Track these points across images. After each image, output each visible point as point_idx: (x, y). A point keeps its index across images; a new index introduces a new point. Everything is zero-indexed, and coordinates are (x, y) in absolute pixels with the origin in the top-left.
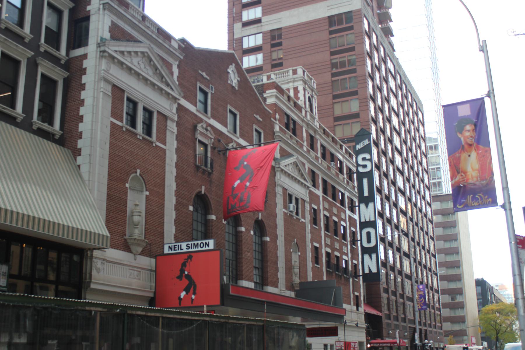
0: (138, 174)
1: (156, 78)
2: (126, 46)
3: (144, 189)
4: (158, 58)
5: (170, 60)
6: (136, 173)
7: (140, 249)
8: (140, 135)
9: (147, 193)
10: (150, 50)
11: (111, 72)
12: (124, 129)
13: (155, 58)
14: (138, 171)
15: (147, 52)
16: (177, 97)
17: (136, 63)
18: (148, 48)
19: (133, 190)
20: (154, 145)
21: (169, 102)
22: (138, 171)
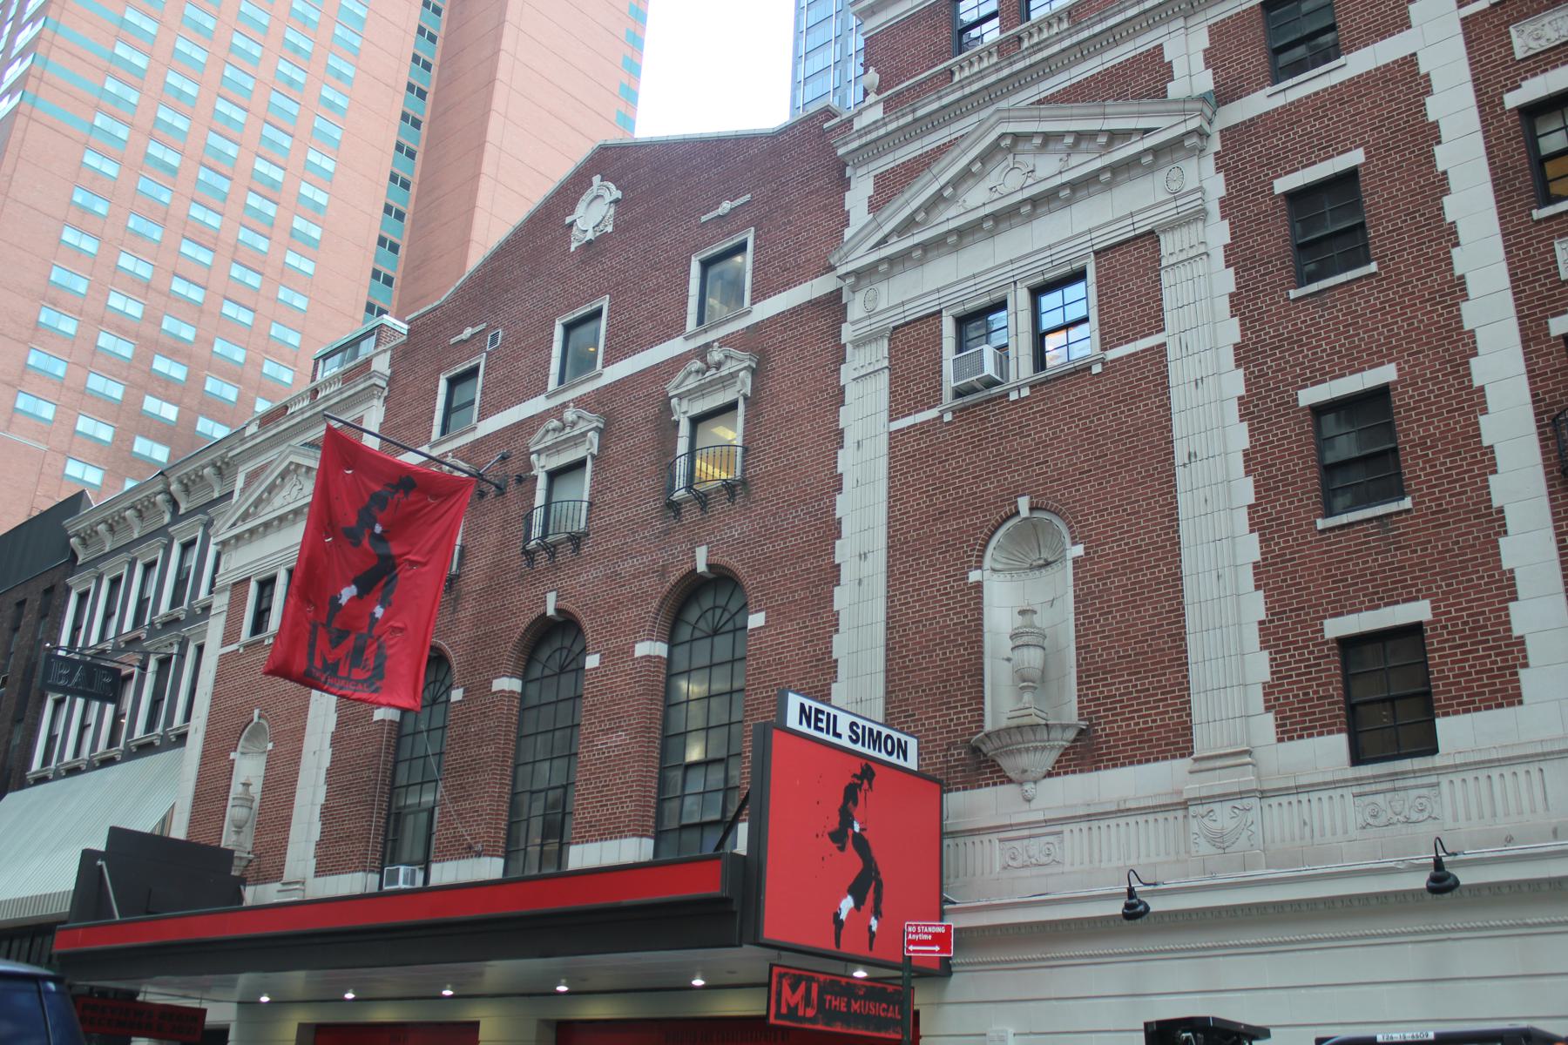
0: (1024, 510)
1: (1075, 159)
2: (907, 202)
3: (1068, 540)
4: (1045, 110)
5: (1144, 43)
6: (1018, 513)
7: (1048, 759)
8: (1019, 389)
9: (1079, 550)
10: (1009, 120)
11: (882, 305)
12: (948, 417)
13: (1040, 119)
14: (1024, 504)
15: (1003, 136)
16: (1181, 129)
17: (977, 199)
18: (1000, 121)
19: (1047, 564)
20: (1097, 369)
21: (1160, 177)
22: (1024, 504)
